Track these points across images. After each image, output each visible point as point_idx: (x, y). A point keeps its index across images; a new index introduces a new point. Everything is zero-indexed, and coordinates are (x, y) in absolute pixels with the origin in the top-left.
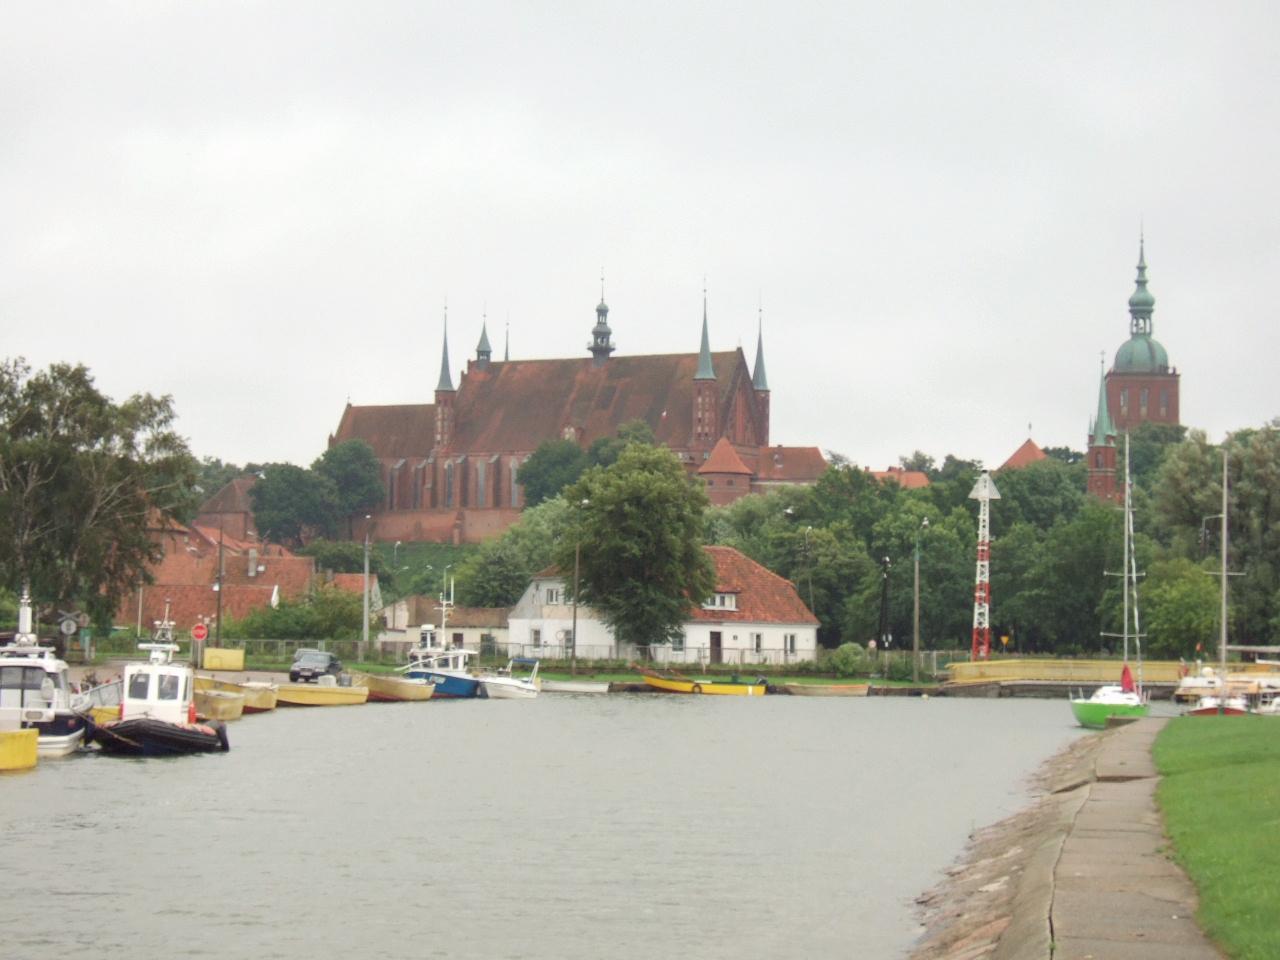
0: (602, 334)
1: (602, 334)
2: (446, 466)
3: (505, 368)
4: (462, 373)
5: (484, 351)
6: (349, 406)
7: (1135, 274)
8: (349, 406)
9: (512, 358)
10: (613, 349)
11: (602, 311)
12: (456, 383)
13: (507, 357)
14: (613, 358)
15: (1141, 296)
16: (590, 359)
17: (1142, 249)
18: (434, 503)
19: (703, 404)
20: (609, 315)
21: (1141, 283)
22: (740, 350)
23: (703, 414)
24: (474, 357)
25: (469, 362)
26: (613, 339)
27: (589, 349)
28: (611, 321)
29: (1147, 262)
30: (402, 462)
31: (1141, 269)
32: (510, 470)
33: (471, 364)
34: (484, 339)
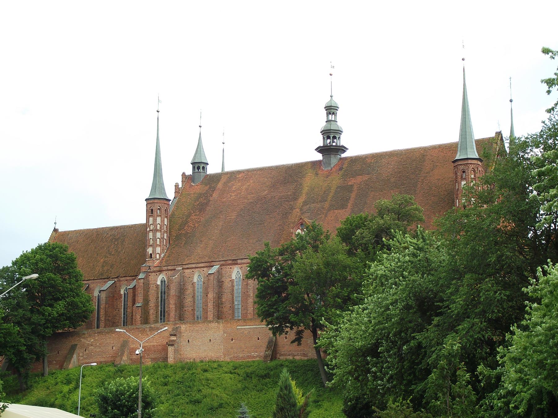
2: (159, 283)
3: (223, 180)
4: (177, 186)
6: (55, 230)
8: (55, 230)
9: (229, 168)
11: (331, 110)
13: (222, 171)
14: (345, 158)
16: (319, 162)
18: (146, 320)
20: (338, 113)
22: (499, 134)
24: (189, 171)
25: (184, 174)
26: (343, 141)
27: (320, 150)
30: (111, 283)
32: (232, 281)
34: (199, 149)
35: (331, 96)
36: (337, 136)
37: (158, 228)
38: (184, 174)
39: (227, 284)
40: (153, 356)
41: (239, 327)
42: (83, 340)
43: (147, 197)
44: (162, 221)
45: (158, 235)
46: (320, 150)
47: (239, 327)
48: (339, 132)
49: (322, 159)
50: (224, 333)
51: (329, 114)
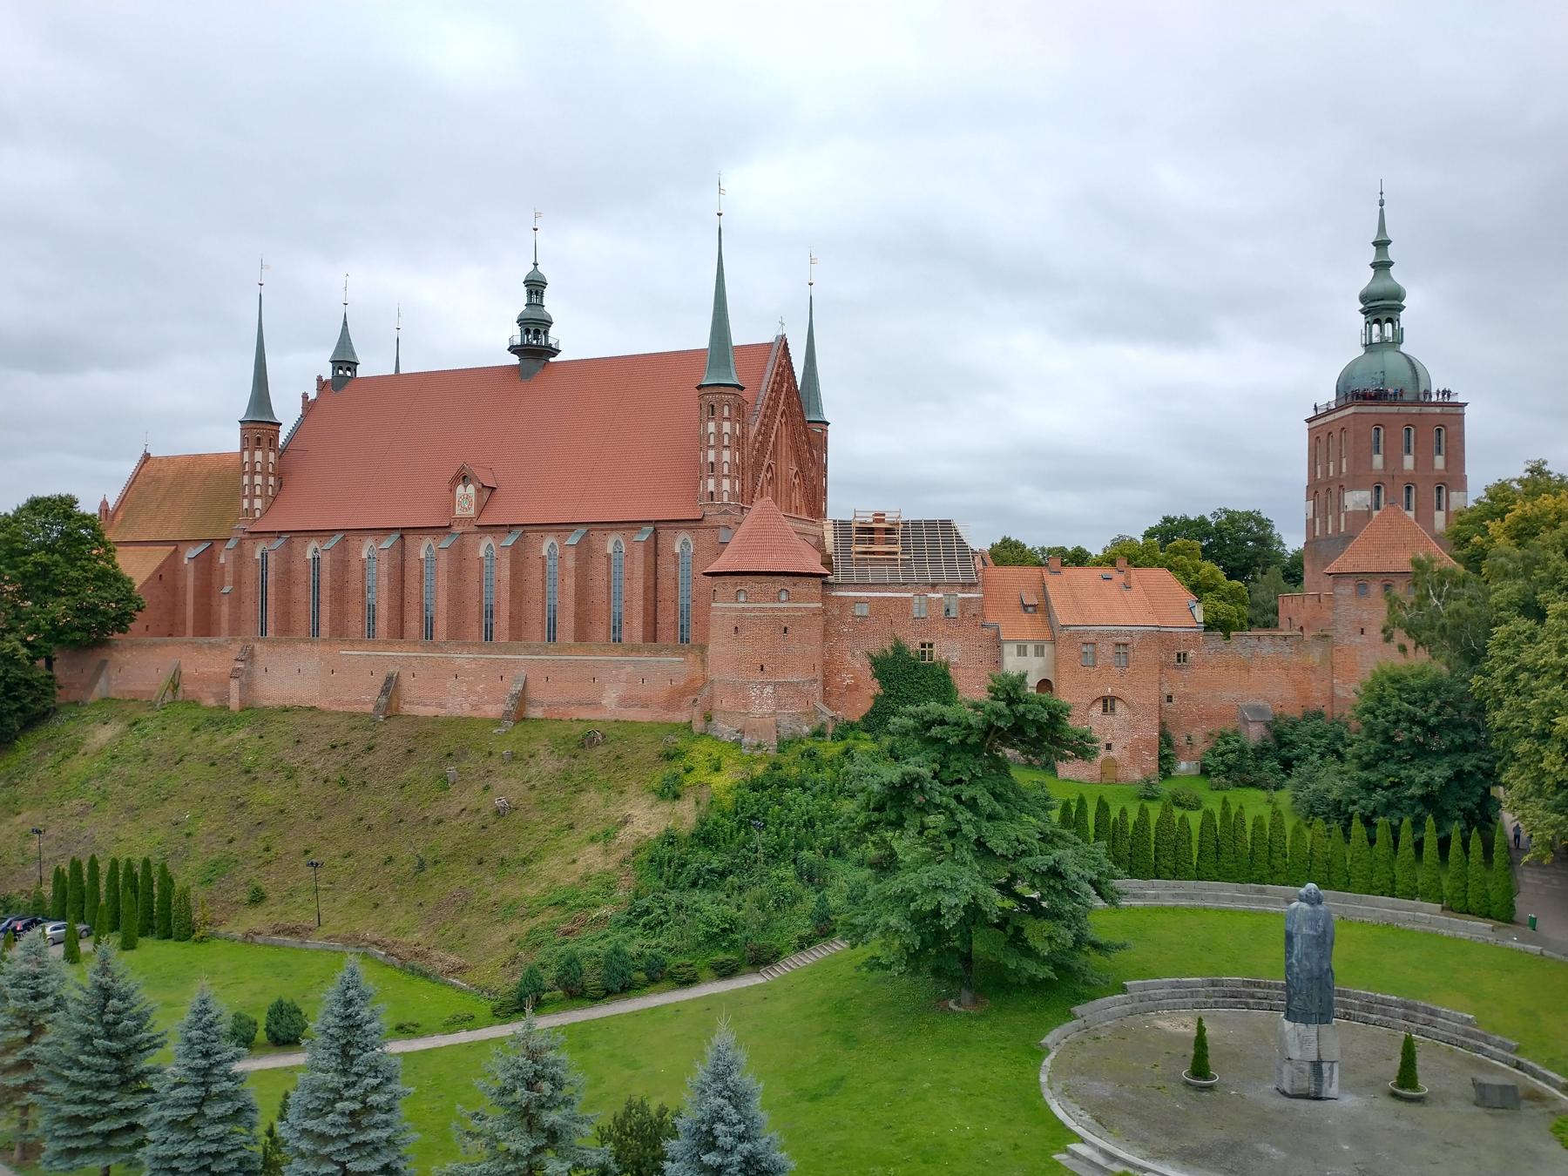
0: (535, 324)
1: (535, 324)
5: (344, 363)
6: (147, 457)
7: (1371, 254)
8: (147, 457)
10: (555, 352)
11: (535, 286)
12: (287, 412)
15: (1381, 286)
17: (1382, 211)
19: (719, 434)
21: (1381, 266)
23: (719, 455)
25: (319, 379)
26: (555, 335)
27: (513, 349)
28: (552, 304)
29: (1390, 234)
31: (1381, 244)
33: (322, 385)
34: (345, 340)
35: (536, 264)
36: (542, 330)
37: (258, 468)
38: (319, 379)
39: (355, 565)
40: (215, 690)
41: (344, 652)
42: (115, 654)
43: (241, 418)
44: (266, 457)
45: (258, 479)
46: (513, 349)
47: (344, 652)
48: (547, 323)
49: (518, 362)
50: (321, 659)
51: (530, 293)
